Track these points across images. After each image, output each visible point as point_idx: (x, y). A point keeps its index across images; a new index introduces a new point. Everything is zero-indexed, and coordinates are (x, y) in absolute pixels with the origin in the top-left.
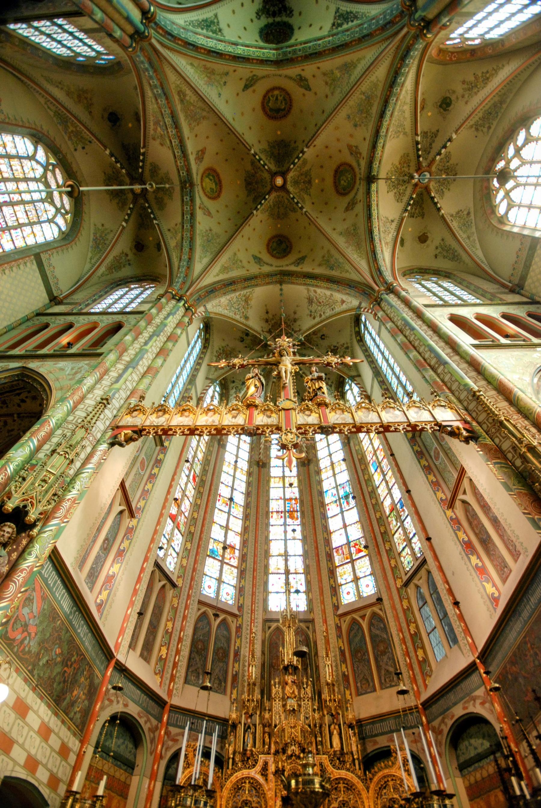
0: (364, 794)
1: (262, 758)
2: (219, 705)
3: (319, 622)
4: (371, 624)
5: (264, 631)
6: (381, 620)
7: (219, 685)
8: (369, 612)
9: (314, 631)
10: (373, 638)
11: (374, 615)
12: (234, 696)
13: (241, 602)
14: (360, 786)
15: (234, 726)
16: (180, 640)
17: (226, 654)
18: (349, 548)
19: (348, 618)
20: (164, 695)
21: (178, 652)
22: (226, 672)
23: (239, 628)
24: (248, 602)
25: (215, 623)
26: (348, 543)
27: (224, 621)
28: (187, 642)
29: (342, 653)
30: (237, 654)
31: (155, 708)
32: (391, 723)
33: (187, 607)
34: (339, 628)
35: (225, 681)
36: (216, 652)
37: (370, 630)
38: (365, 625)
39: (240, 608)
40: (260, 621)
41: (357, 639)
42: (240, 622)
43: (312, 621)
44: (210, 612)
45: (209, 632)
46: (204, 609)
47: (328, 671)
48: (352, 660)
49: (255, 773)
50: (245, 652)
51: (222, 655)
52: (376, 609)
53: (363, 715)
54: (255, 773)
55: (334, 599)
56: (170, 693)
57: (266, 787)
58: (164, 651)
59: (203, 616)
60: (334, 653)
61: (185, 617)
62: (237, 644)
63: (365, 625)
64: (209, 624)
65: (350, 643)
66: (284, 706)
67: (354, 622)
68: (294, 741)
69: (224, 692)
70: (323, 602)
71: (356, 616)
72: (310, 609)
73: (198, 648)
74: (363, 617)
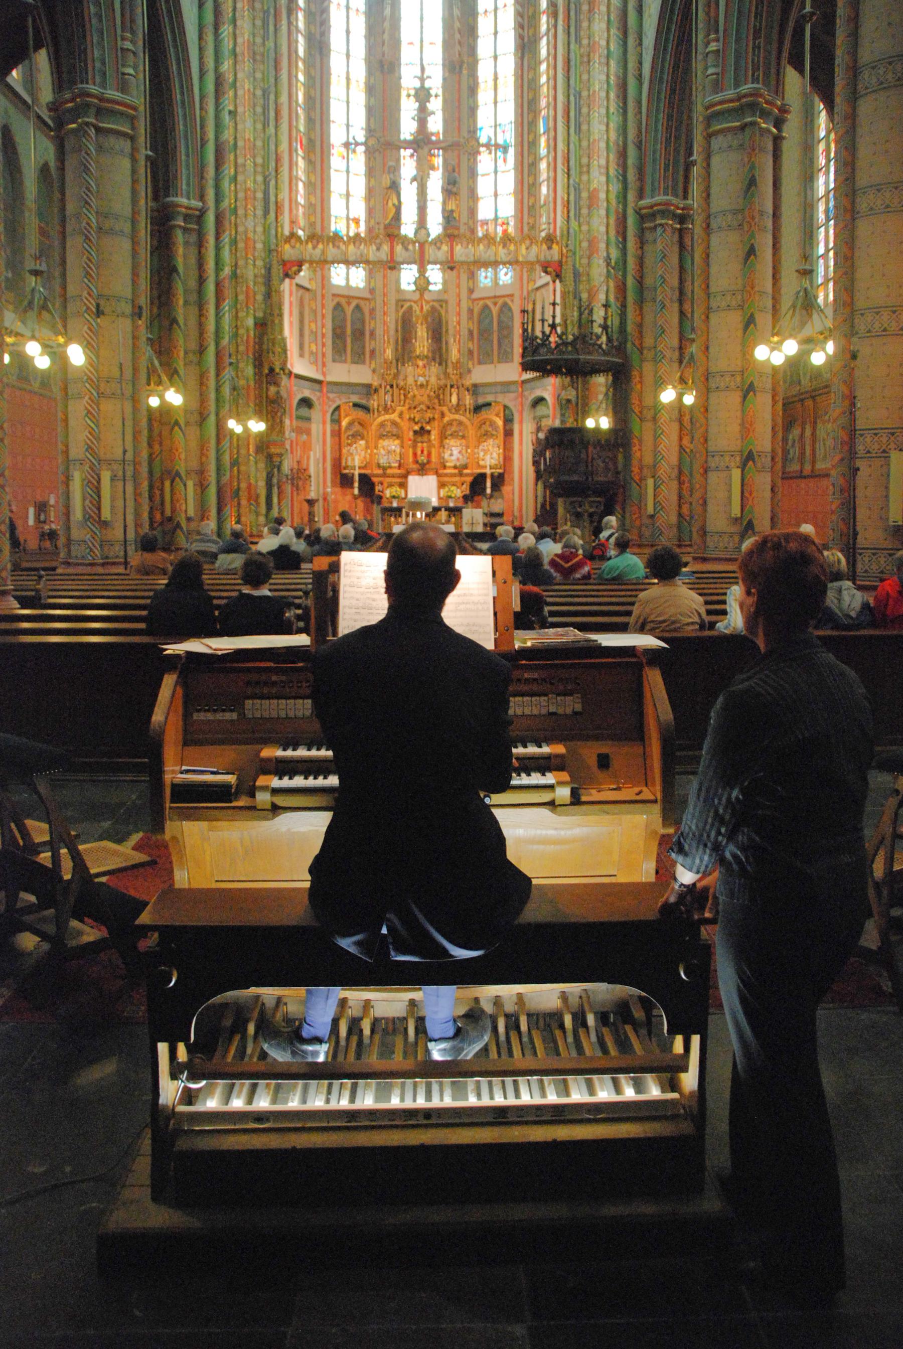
0: (470, 427)
1: (399, 409)
2: (361, 374)
3: (452, 303)
4: (501, 311)
5: (397, 311)
6: (510, 310)
7: (359, 357)
8: (501, 301)
9: (447, 311)
10: (499, 323)
11: (505, 304)
12: (373, 366)
13: (372, 284)
14: (468, 423)
15: (376, 391)
16: (323, 336)
17: (362, 333)
18: (496, 225)
19: (481, 302)
20: (320, 378)
21: (324, 345)
22: (364, 347)
23: (372, 311)
24: (379, 285)
25: (349, 310)
26: (496, 219)
27: (358, 307)
28: (329, 335)
29: (471, 333)
30: (372, 334)
31: (317, 386)
32: (499, 388)
33: (323, 306)
34: (470, 311)
35: (364, 354)
36: (354, 333)
37: (499, 316)
38: (495, 310)
39: (372, 291)
40: (393, 302)
41: (487, 321)
42: (372, 305)
43: (446, 302)
44: (343, 301)
45: (345, 320)
46: (337, 300)
47: (454, 354)
48: (479, 340)
49: (394, 416)
50: (379, 332)
51: (359, 334)
52: (508, 300)
53: (478, 381)
54: (394, 416)
55: (471, 282)
56: (324, 374)
57: (402, 424)
58: (314, 348)
59: (338, 306)
60: (464, 332)
61: (323, 316)
62: (372, 325)
63: (495, 310)
64: (343, 311)
65: (480, 322)
66: (416, 381)
67: (486, 307)
68: (422, 403)
69: (364, 362)
70: (458, 286)
71: (489, 303)
72: (445, 291)
73: (338, 334)
74: (495, 304)
